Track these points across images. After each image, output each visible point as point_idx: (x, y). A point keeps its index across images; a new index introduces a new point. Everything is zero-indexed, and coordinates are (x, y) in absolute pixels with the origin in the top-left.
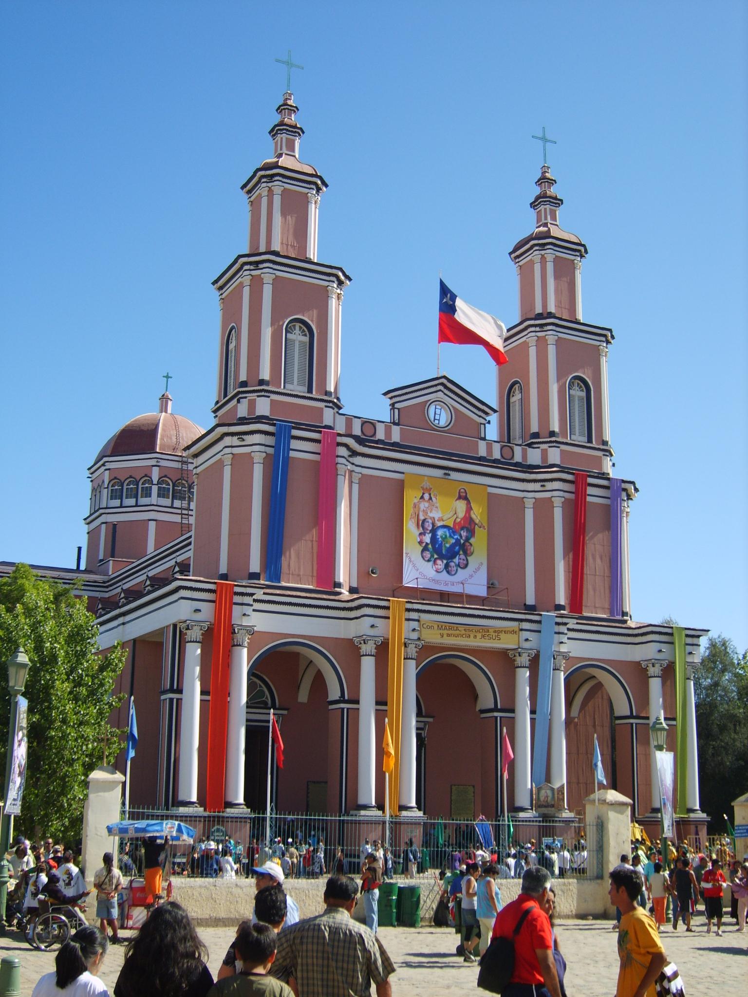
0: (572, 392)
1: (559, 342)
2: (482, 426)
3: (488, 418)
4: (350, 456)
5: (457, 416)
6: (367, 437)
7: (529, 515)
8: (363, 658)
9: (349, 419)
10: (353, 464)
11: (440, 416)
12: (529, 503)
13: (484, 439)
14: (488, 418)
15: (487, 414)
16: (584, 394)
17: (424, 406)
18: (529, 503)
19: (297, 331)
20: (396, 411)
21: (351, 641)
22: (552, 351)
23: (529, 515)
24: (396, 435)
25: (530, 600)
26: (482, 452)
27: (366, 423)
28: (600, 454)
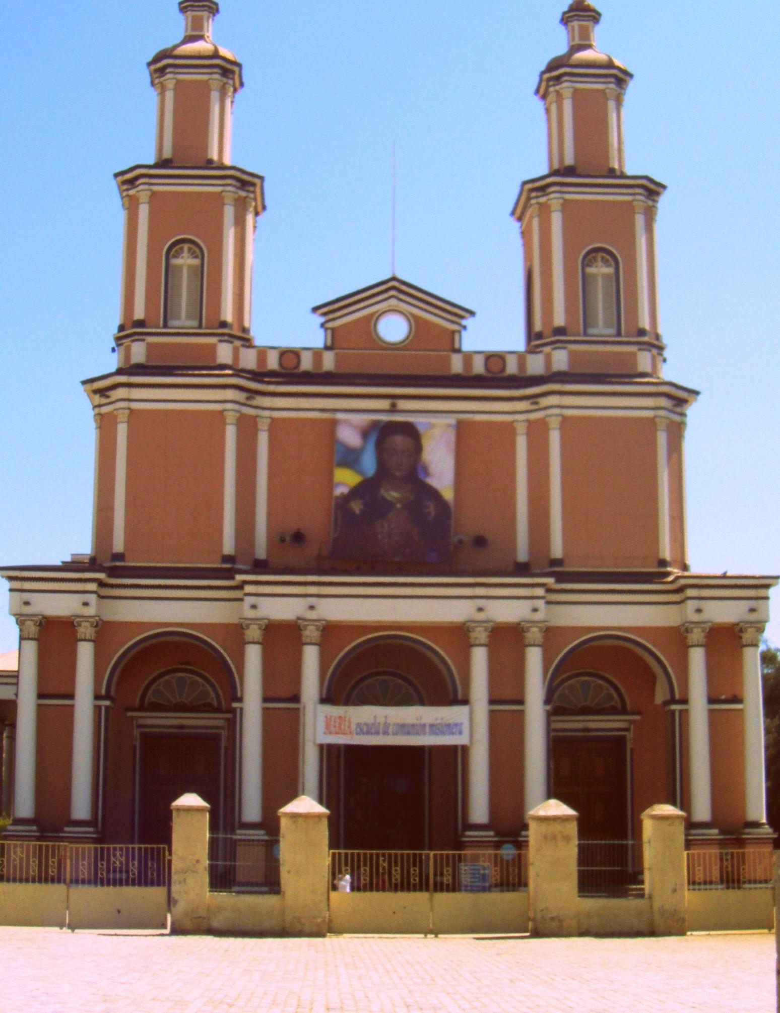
0: (590, 270)
1: (566, 206)
2: (457, 336)
3: (464, 322)
4: (248, 398)
5: (417, 325)
6: (290, 371)
7: (521, 444)
8: (247, 646)
9: (262, 353)
10: (257, 407)
11: (393, 329)
12: (521, 429)
13: (459, 351)
14: (464, 322)
15: (462, 317)
16: (610, 270)
17: (370, 322)
18: (521, 429)
19: (186, 254)
20: (329, 332)
21: (235, 625)
22: (556, 219)
23: (521, 444)
24: (329, 362)
25: (522, 555)
26: (457, 365)
27: (285, 353)
28: (633, 349)
